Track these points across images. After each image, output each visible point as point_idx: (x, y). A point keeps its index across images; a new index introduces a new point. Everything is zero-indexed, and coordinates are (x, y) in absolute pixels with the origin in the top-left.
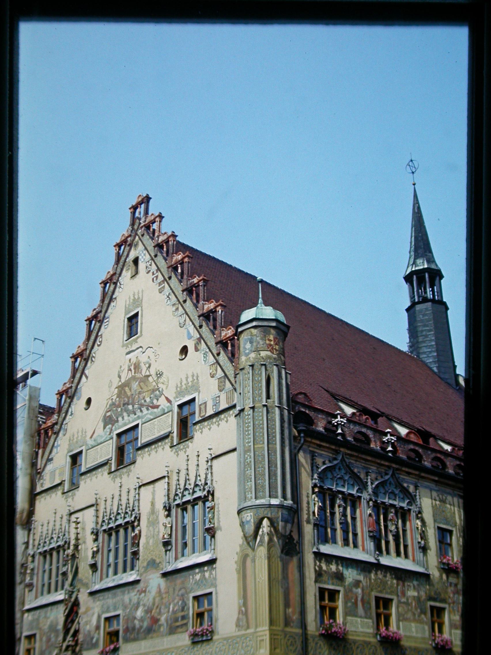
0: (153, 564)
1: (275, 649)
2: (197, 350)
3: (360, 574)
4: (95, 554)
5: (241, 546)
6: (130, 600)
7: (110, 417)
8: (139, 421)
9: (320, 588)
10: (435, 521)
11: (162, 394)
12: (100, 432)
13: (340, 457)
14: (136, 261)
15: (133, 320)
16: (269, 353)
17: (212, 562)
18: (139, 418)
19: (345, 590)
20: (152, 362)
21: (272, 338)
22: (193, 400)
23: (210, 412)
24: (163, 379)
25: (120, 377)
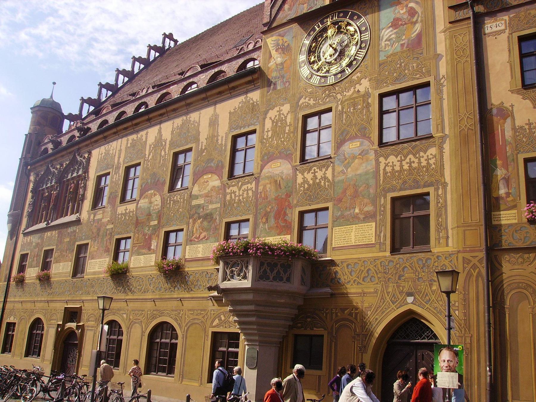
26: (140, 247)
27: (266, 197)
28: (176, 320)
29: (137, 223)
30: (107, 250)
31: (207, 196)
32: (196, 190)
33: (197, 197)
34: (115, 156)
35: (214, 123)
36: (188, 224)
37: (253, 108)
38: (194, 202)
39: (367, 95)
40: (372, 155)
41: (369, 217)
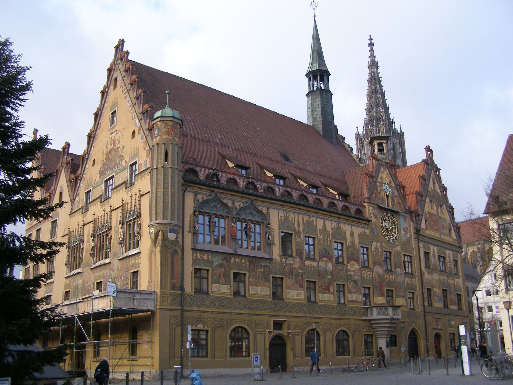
0: (116, 254)
1: (163, 302)
2: (139, 134)
3: (223, 260)
4: (93, 248)
5: (150, 246)
6: (106, 273)
7: (103, 171)
8: (114, 174)
9: (195, 269)
10: (279, 228)
11: (124, 158)
12: (98, 179)
13: (214, 194)
14: (116, 79)
15: (114, 113)
16: (167, 136)
17: (139, 253)
18: (114, 172)
19: (212, 269)
20: (121, 140)
21: (169, 127)
22: (136, 163)
23: (143, 169)
24: (124, 150)
25: (107, 148)
26: (323, 289)
27: (376, 280)
28: (348, 329)
29: (319, 275)
30: (301, 286)
31: (354, 271)
32: (349, 267)
33: (350, 271)
34: (295, 223)
35: (352, 234)
36: (347, 283)
37: (367, 237)
38: (349, 273)
39: (400, 253)
40: (403, 276)
41: (404, 297)
